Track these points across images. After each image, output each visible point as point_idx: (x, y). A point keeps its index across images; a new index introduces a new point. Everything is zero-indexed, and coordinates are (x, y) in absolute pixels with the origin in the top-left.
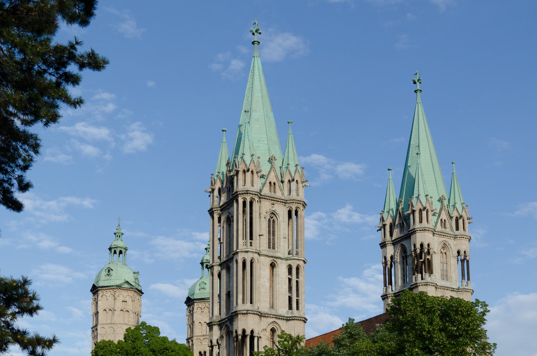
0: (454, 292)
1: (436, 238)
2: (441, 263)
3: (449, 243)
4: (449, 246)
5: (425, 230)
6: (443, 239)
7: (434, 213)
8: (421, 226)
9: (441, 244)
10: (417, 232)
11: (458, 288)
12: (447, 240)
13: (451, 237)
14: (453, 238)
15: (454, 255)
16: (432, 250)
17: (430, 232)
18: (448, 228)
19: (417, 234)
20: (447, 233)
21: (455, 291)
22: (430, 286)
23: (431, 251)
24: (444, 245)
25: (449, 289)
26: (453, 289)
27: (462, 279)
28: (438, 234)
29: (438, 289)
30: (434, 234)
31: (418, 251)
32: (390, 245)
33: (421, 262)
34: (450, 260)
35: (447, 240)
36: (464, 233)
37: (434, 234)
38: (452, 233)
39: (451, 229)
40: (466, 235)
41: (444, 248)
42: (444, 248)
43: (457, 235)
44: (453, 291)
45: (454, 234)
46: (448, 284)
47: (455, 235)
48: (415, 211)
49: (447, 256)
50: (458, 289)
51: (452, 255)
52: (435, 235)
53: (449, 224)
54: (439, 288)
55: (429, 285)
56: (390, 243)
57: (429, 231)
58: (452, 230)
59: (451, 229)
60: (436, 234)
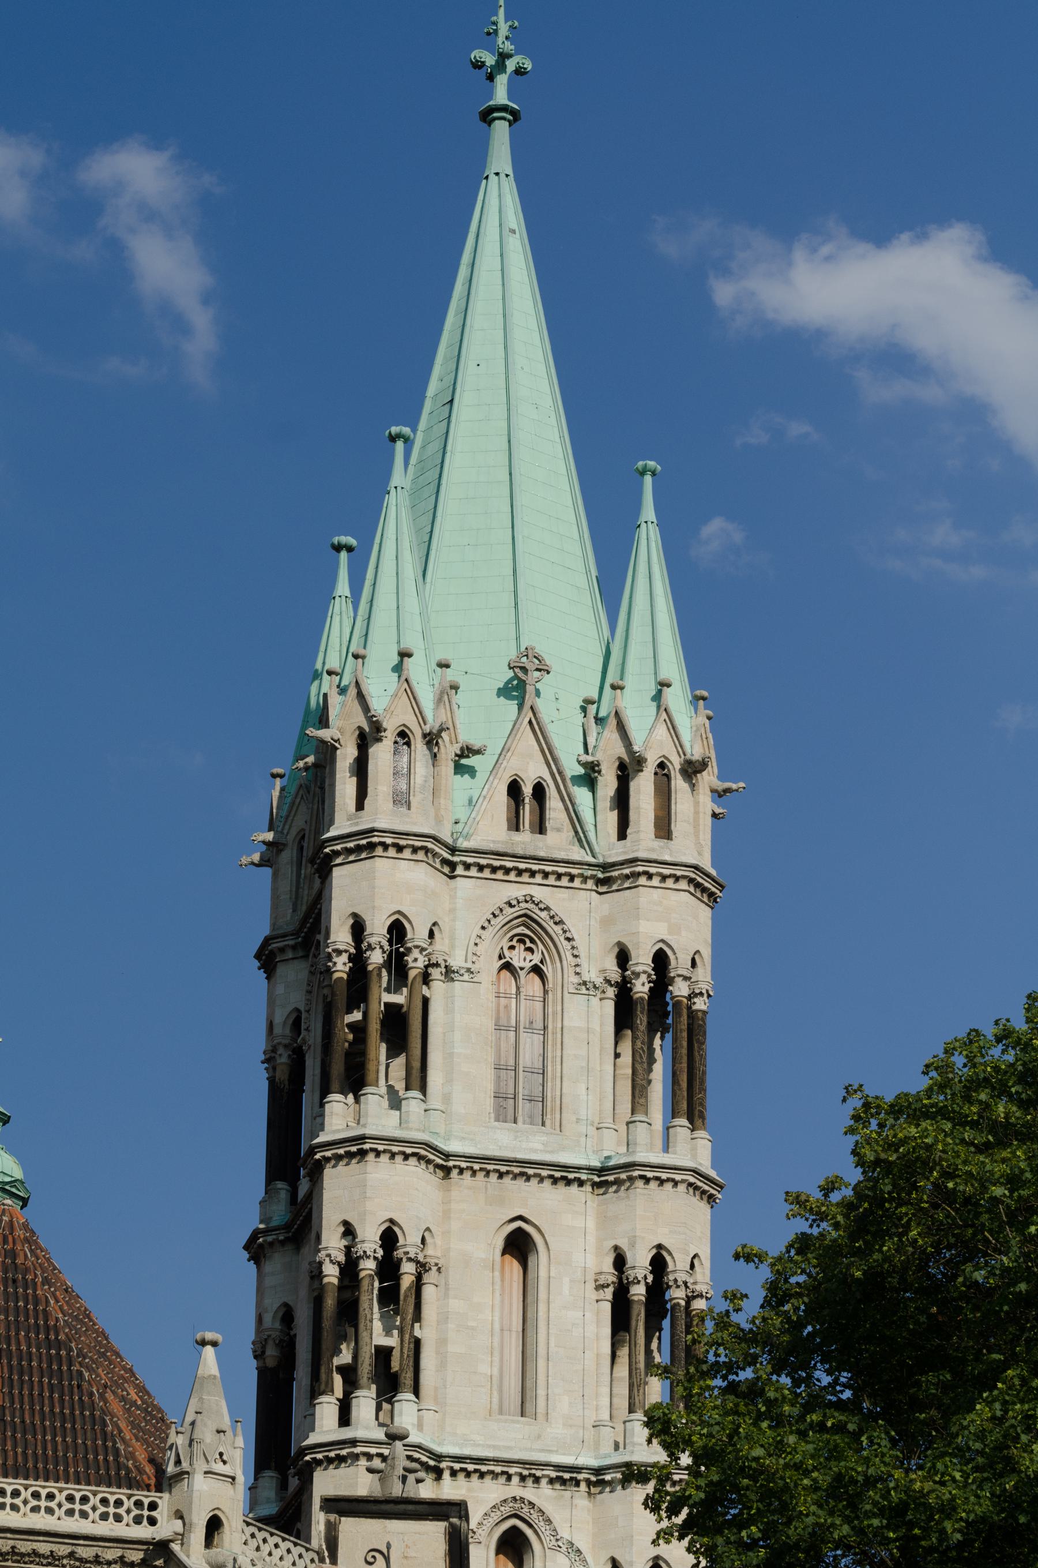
0: (574, 1188)
1: (466, 886)
2: (499, 1027)
3: (555, 909)
4: (555, 930)
5: (371, 846)
6: (516, 891)
7: (459, 752)
8: (357, 824)
9: (501, 920)
10: (339, 861)
11: (598, 1164)
12: (539, 893)
13: (572, 878)
14: (590, 884)
15: (586, 977)
16: (416, 953)
17: (407, 853)
18: (558, 830)
19: (336, 872)
20: (542, 854)
21: (581, 1183)
22: (384, 1158)
23: (416, 962)
24: (524, 925)
25: (530, 1172)
26: (565, 1168)
27: (633, 1112)
28: (481, 868)
29: (455, 1173)
30: (453, 866)
31: (341, 966)
32: (290, 954)
33: (350, 1026)
34: (559, 1008)
35: (539, 893)
36: (653, 850)
37: (453, 866)
38: (578, 854)
39: (576, 832)
40: (667, 858)
41: (532, 941)
42: (529, 944)
43: (610, 860)
44: (568, 1182)
45: (590, 859)
46: (539, 1146)
47: (605, 867)
48: (337, 749)
49: (550, 985)
50: (602, 1171)
51: (576, 980)
52: (460, 870)
53: (560, 805)
54: (461, 1171)
55: (378, 1154)
56: (294, 948)
57: (400, 849)
58: (581, 838)
59: (576, 832)
60: (467, 866)
